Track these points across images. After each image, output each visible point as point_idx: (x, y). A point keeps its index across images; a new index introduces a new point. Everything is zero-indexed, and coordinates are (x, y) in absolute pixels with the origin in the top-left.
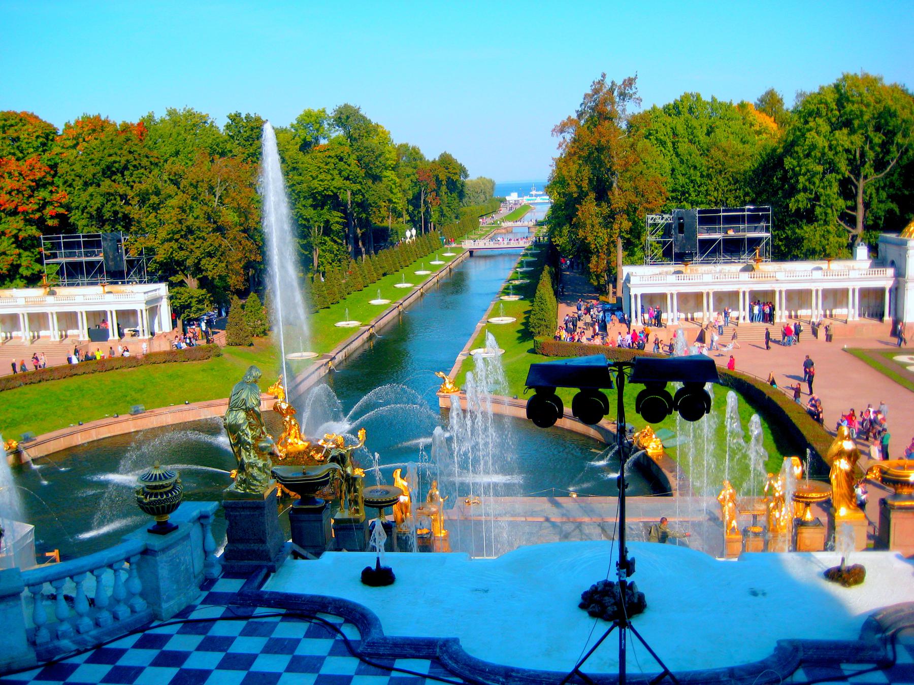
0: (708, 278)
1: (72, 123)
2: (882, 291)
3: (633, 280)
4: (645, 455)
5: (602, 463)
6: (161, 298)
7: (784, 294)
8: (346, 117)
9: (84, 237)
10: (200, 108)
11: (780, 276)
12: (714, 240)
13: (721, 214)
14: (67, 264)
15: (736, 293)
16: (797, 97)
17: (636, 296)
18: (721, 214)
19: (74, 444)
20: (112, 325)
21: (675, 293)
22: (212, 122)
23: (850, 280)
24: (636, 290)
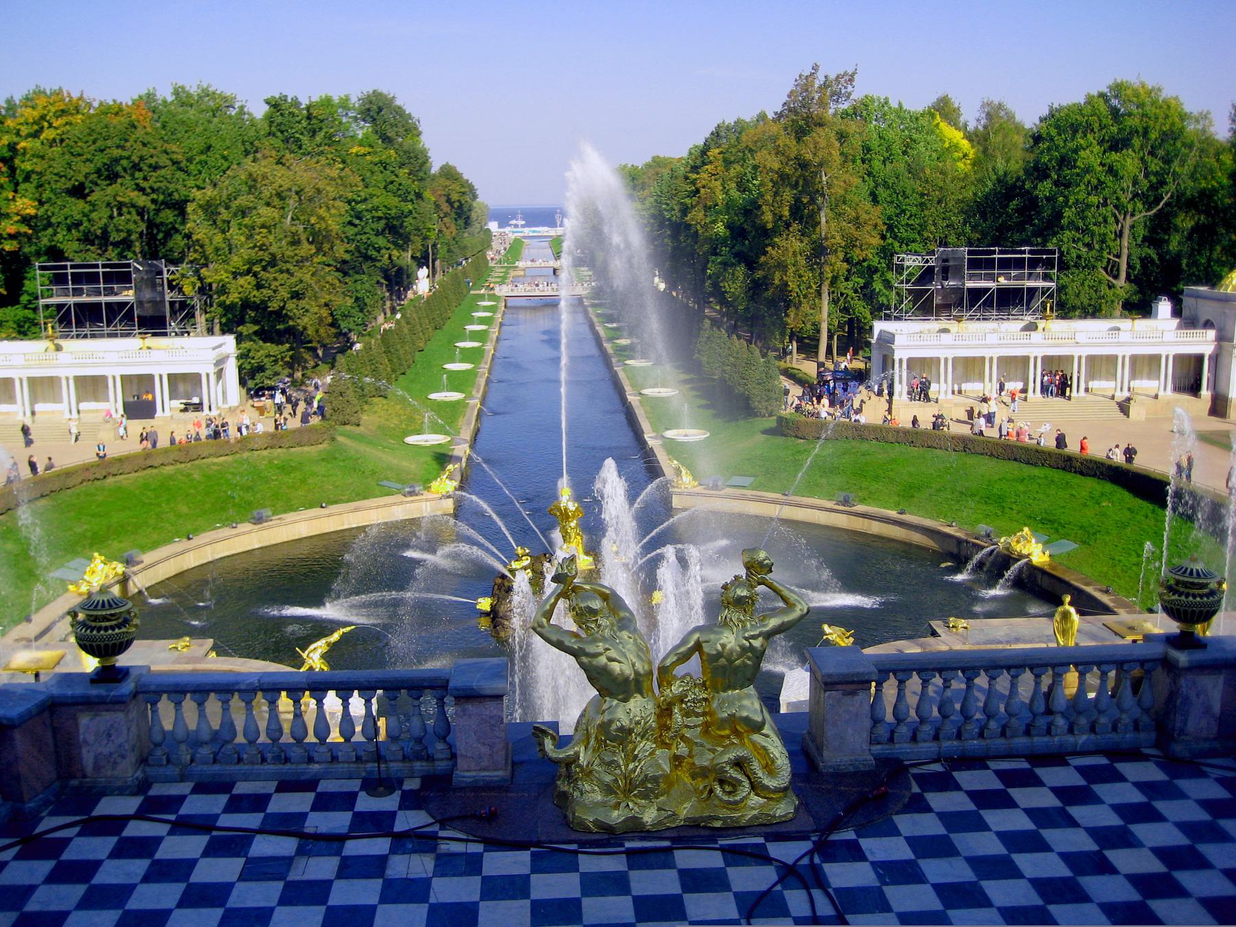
0: (992, 339)
1: (17, 99)
2: (1199, 359)
3: (899, 341)
4: (1029, 565)
5: (959, 578)
6: (228, 357)
7: (1083, 360)
8: (378, 111)
9: (104, 266)
10: (222, 85)
11: (1080, 338)
12: (987, 290)
13: (996, 256)
14: (76, 305)
15: (1026, 359)
16: (983, 106)
17: (901, 361)
18: (996, 256)
19: (185, 568)
20: (161, 392)
21: (950, 357)
22: (242, 107)
23: (1163, 344)
24: (901, 353)
